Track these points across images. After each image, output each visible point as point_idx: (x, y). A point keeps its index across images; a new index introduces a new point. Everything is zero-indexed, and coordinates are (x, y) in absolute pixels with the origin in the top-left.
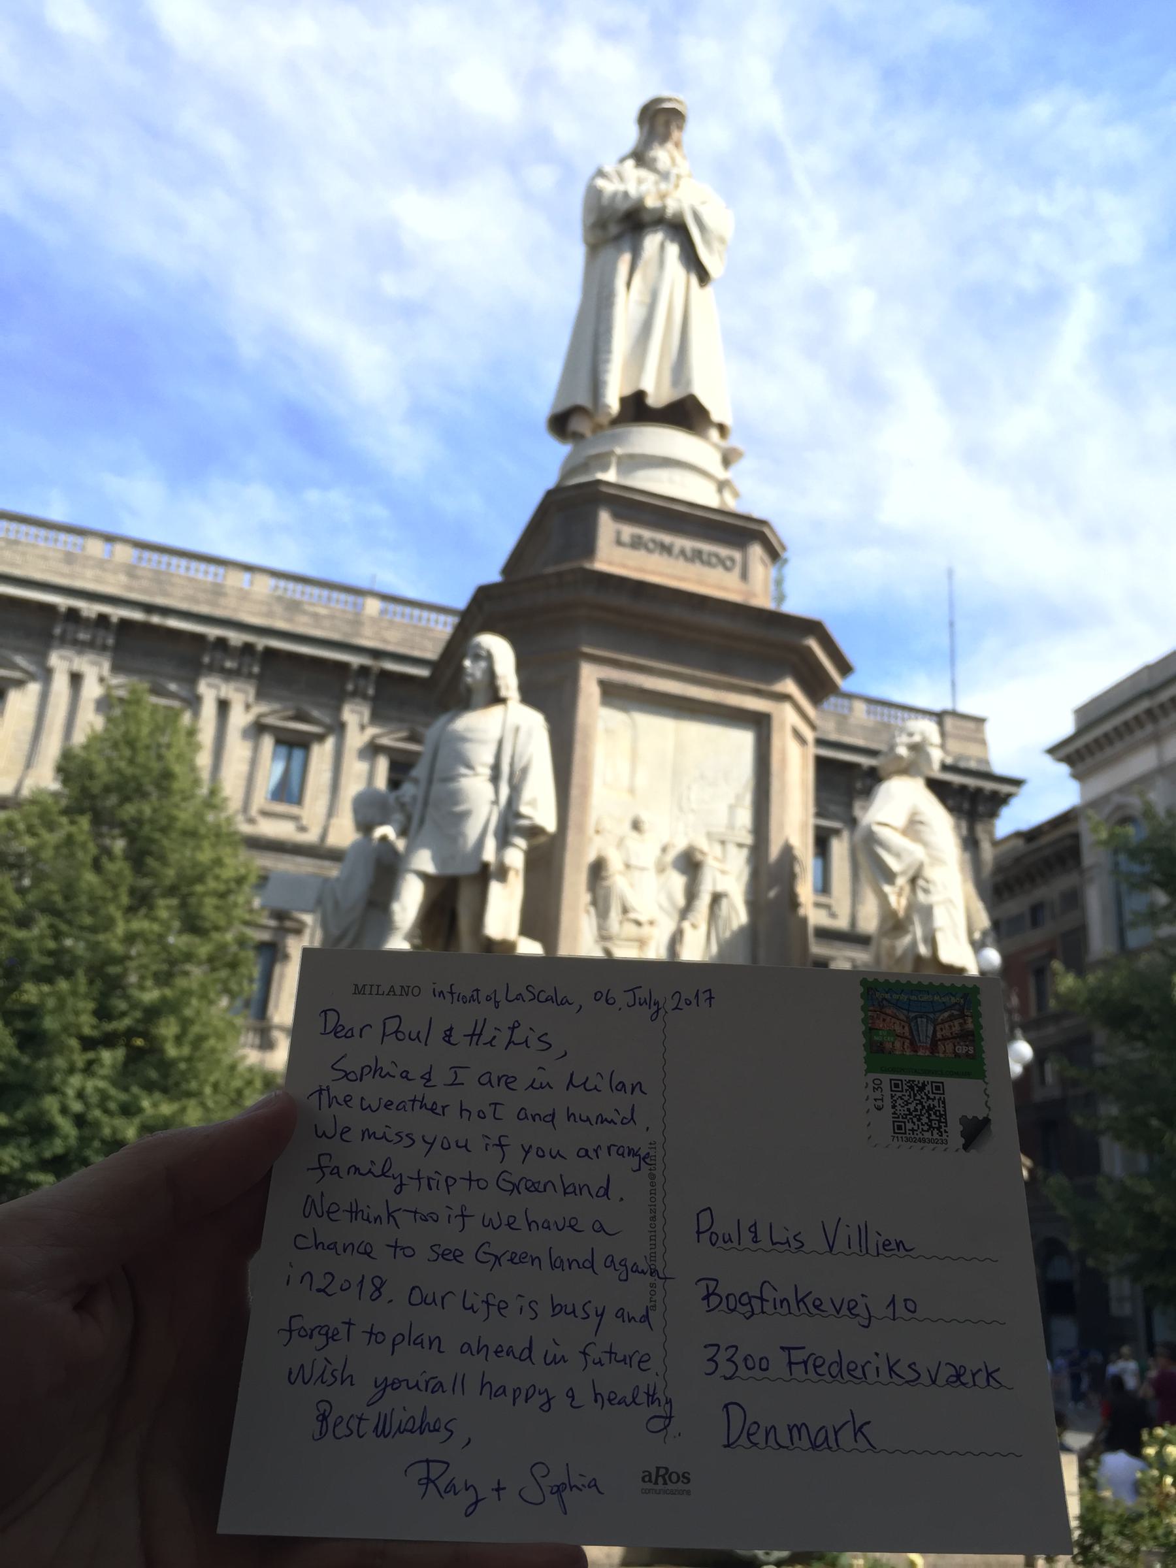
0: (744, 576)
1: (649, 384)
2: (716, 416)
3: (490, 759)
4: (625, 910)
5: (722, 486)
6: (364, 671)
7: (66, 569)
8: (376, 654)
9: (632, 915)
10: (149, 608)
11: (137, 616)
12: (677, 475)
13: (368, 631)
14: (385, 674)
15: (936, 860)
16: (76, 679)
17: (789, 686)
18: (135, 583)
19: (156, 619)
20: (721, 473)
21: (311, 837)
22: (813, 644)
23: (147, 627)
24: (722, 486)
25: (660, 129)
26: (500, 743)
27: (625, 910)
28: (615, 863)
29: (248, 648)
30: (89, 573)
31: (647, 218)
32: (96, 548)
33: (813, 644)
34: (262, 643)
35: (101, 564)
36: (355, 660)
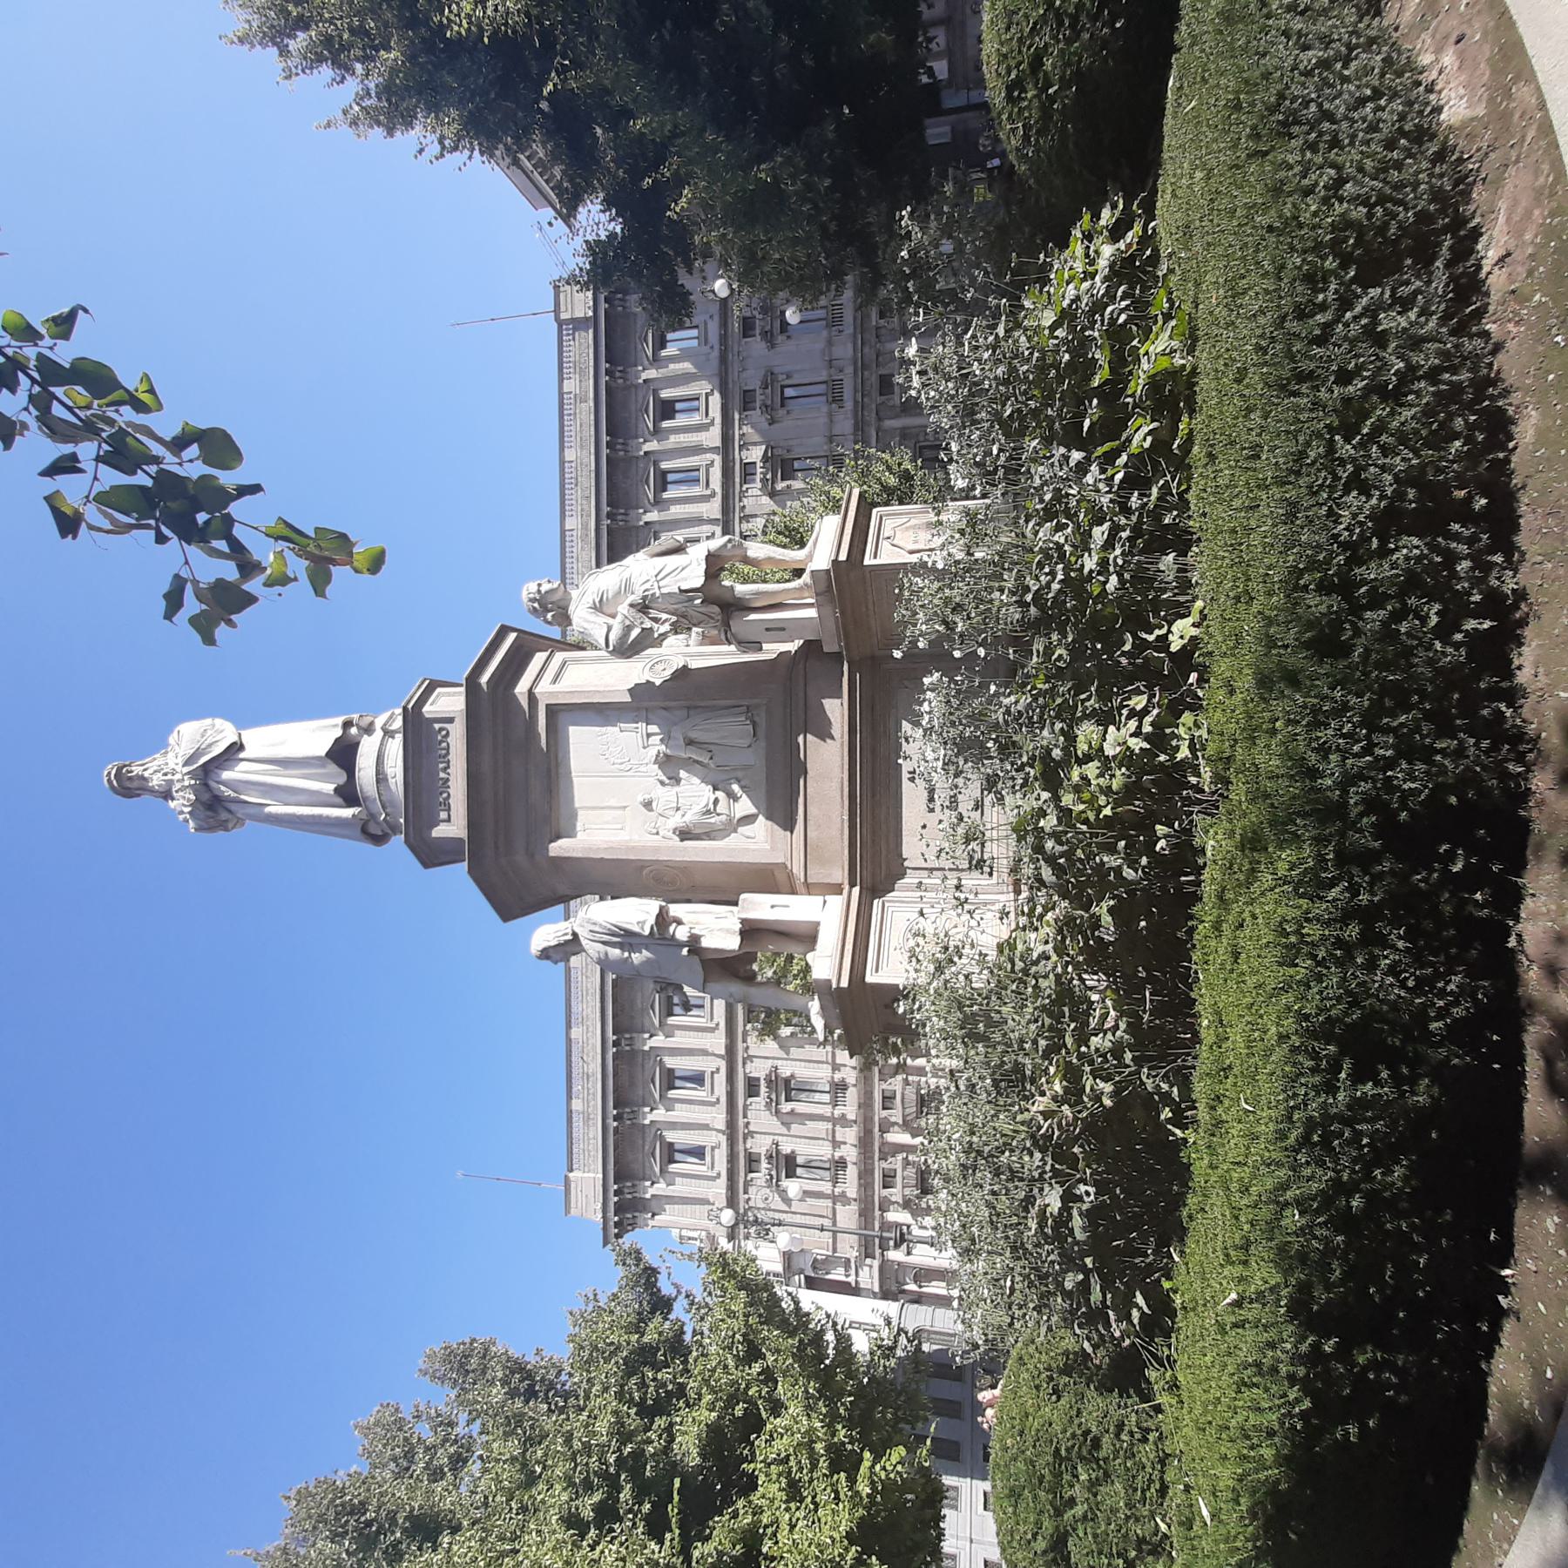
0: (451, 720)
1: (329, 788)
2: (339, 732)
3: (617, 952)
4: (708, 812)
5: (388, 733)
9: (711, 806)
12: (389, 771)
15: (627, 587)
17: (521, 688)
20: (379, 734)
22: (484, 679)
24: (388, 733)
25: (135, 784)
26: (604, 943)
27: (708, 812)
28: (677, 821)
31: (206, 797)
33: (484, 679)
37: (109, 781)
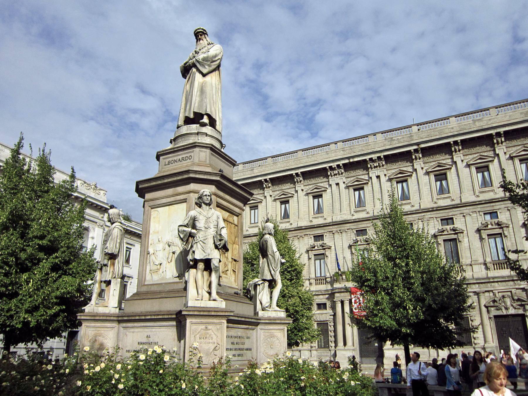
2: (204, 113)
6: (416, 151)
7: (327, 156)
8: (418, 144)
10: (349, 158)
11: (347, 161)
13: (415, 137)
14: (423, 149)
16: (378, 177)
18: (345, 153)
19: (351, 160)
21: (417, 207)
23: (350, 163)
29: (379, 158)
30: (333, 155)
32: (333, 146)
34: (382, 155)
35: (335, 151)
36: (412, 148)
37: (197, 30)
